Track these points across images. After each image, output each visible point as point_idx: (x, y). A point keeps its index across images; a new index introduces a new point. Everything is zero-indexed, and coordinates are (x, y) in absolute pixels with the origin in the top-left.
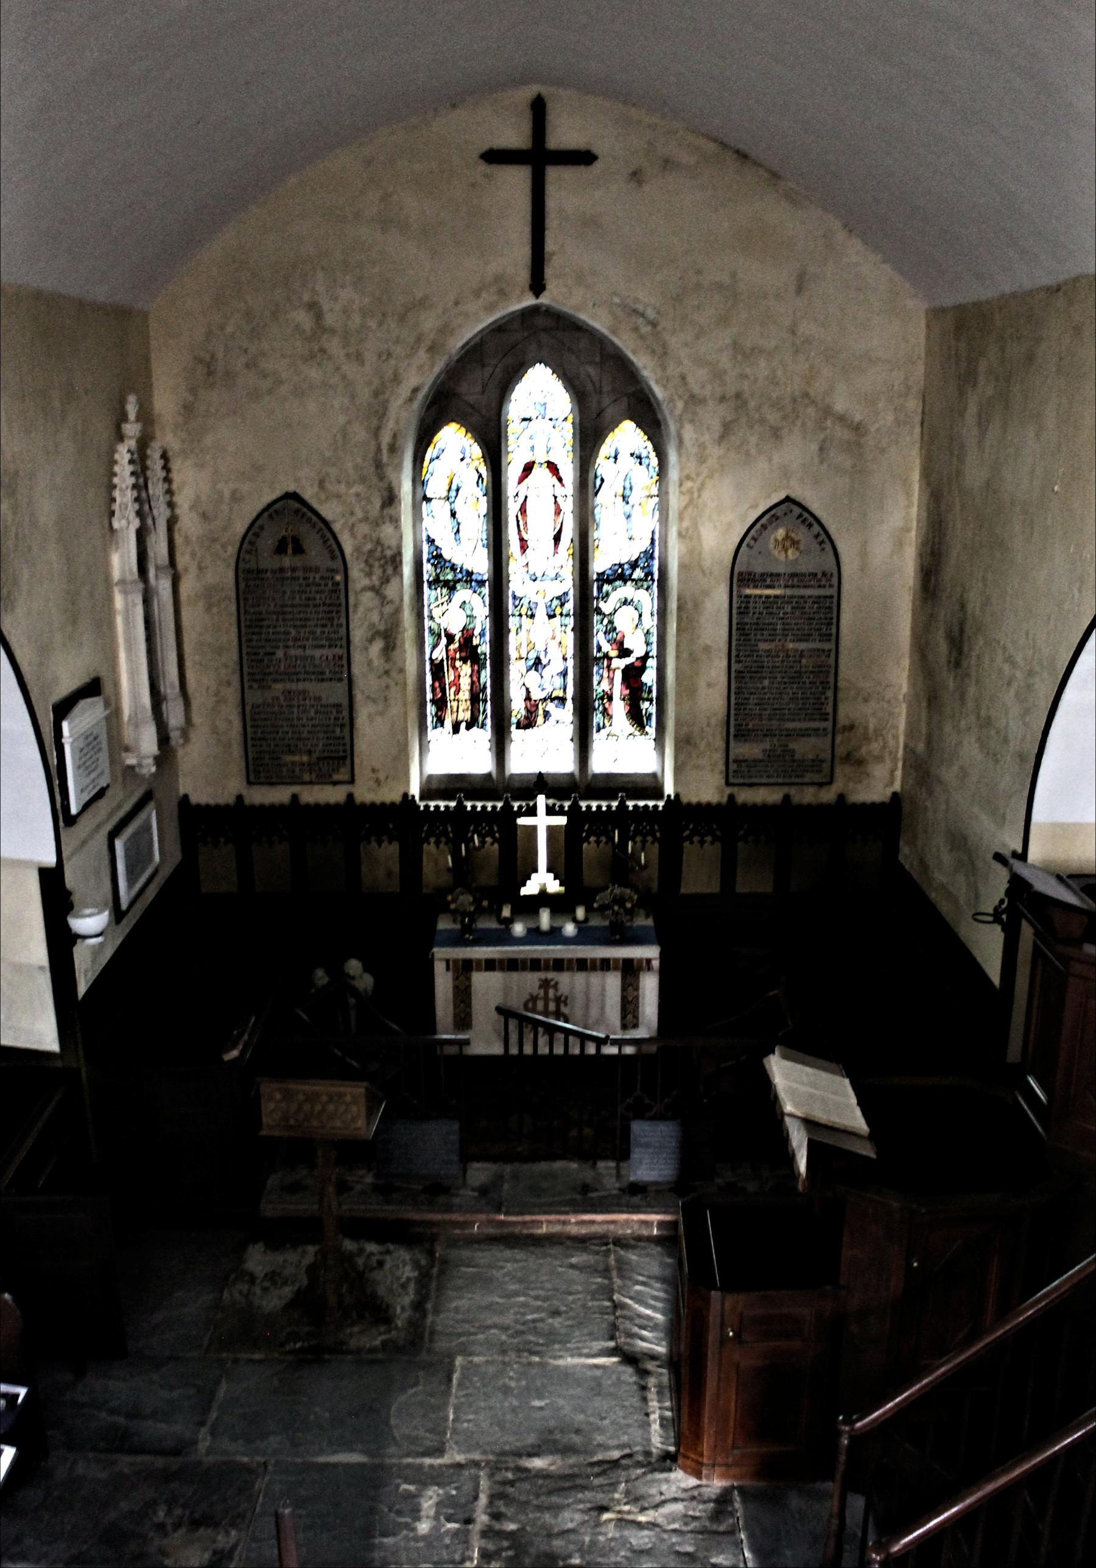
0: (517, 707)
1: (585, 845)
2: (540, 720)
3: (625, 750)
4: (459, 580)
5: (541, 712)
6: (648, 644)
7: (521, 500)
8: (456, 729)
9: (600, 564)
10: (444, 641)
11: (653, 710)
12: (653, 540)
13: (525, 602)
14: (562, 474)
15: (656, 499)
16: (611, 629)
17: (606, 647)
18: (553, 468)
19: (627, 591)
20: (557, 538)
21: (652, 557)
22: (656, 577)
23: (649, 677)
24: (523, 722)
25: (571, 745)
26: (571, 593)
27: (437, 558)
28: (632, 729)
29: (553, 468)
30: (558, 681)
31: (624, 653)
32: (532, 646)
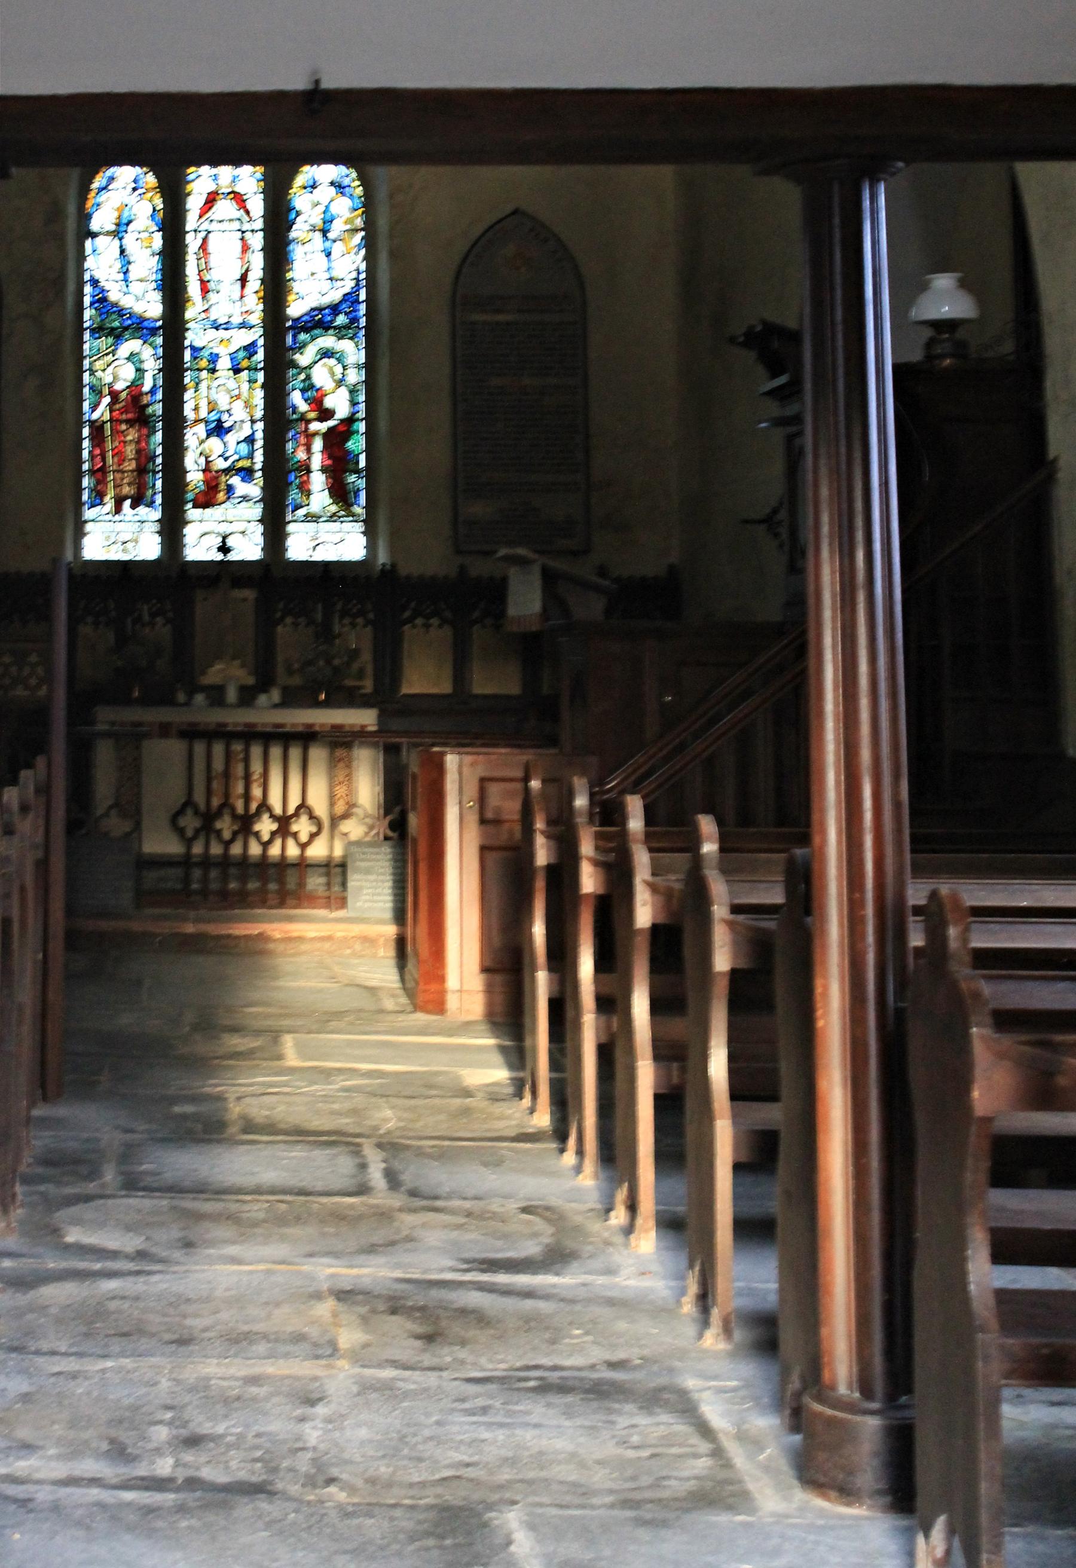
0: (195, 477)
1: (280, 629)
2: (221, 496)
3: (328, 537)
4: (126, 328)
5: (223, 486)
6: (354, 403)
7: (203, 234)
8: (118, 509)
9: (295, 309)
10: (107, 400)
11: (362, 483)
12: (357, 280)
13: (205, 353)
14: (249, 205)
15: (363, 233)
16: (308, 386)
17: (303, 407)
18: (239, 199)
19: (327, 341)
20: (243, 280)
21: (357, 301)
22: (363, 322)
23: (357, 444)
24: (201, 499)
25: (260, 528)
26: (261, 342)
27: (101, 301)
28: (334, 508)
29: (239, 199)
30: (244, 449)
31: (326, 414)
32: (212, 406)
